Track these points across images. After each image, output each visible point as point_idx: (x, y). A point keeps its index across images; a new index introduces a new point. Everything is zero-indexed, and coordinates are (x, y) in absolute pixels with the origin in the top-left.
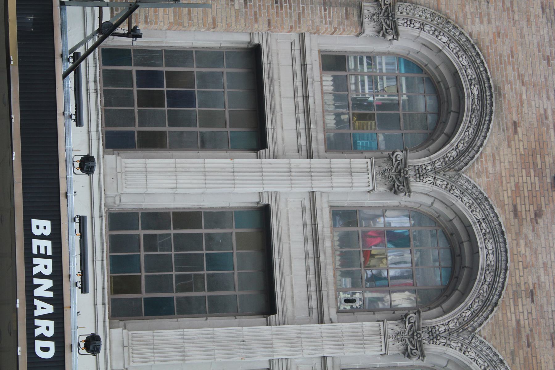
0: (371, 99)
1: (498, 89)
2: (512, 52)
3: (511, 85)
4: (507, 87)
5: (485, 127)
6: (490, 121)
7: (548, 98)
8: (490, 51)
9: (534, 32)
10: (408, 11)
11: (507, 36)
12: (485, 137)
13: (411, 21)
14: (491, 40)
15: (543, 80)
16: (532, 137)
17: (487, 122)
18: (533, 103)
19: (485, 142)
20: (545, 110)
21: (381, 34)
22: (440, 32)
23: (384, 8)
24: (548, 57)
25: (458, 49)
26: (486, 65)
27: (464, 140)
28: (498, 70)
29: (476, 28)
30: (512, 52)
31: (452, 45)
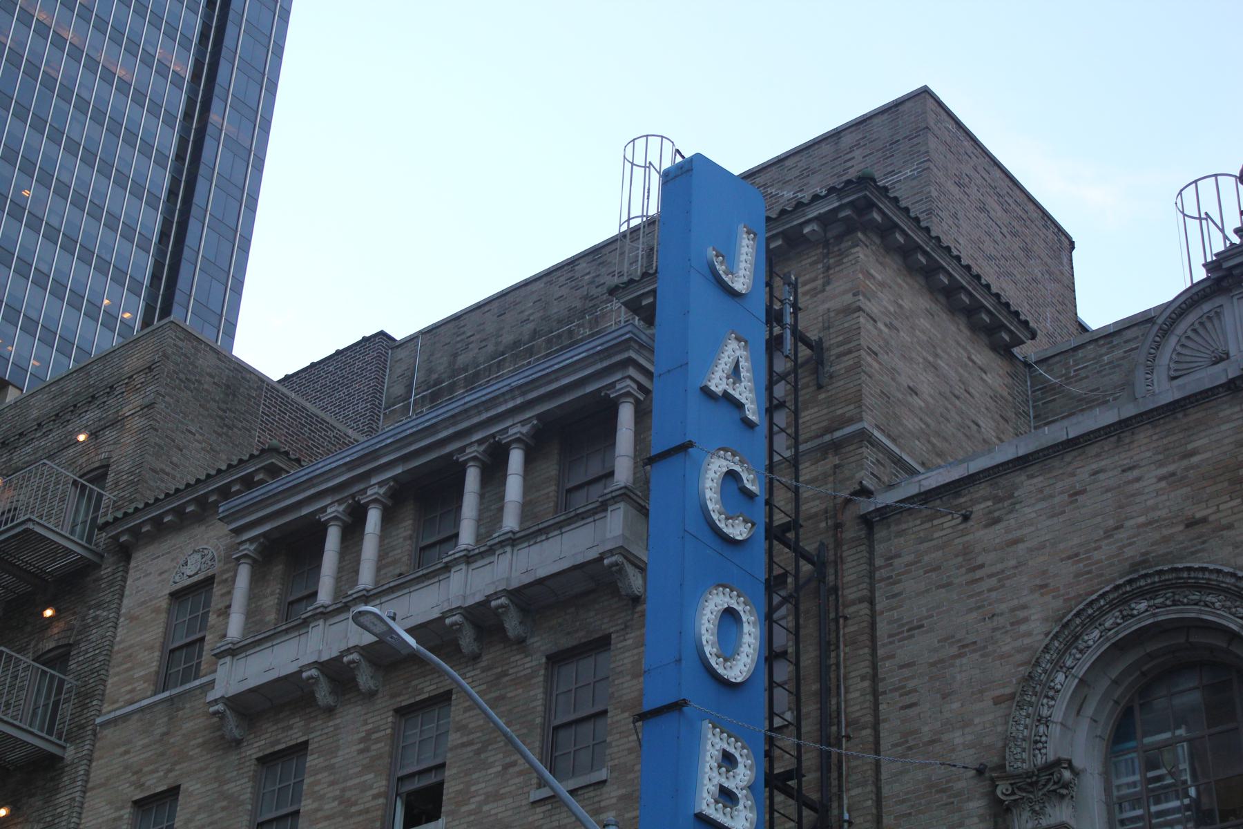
0: (1192, 792)
1: (1134, 567)
2: (1069, 558)
3: (1124, 546)
4: (1129, 552)
5: (1200, 575)
6: (1189, 569)
7: (1138, 479)
8: (1072, 594)
9: (1033, 529)
10: (1019, 750)
11: (1044, 572)
12: (1219, 572)
13: (1036, 742)
14: (1054, 597)
15: (1109, 495)
16: (1208, 490)
17: (1192, 575)
18: (1150, 503)
19: (1226, 569)
20: (1160, 479)
21: (1064, 791)
22: (1051, 688)
23: (1019, 795)
24: (1071, 496)
25: (1074, 651)
26: (1094, 597)
27: (1230, 608)
28: (1102, 575)
29: (1037, 628)
30: (1069, 558)
31: (1069, 663)
